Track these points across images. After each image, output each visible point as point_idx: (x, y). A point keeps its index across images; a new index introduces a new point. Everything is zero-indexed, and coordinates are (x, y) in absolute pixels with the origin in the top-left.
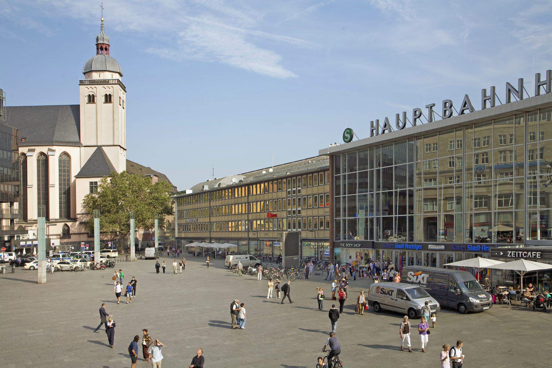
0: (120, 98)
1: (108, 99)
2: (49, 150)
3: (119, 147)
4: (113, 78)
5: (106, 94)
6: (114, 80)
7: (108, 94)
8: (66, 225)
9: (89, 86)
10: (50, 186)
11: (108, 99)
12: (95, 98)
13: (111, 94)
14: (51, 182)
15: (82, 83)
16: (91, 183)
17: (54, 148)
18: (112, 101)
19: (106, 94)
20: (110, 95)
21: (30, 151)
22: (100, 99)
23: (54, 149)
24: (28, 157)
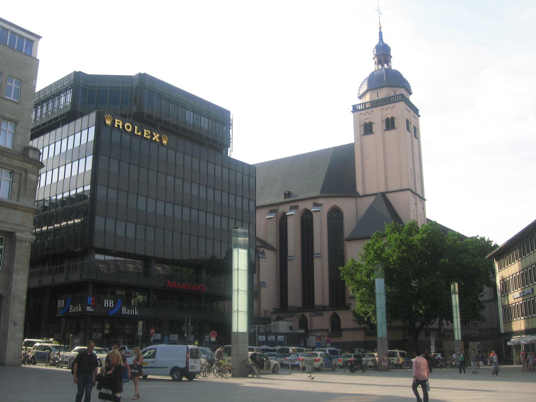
0: (408, 122)
1: (390, 124)
2: (315, 205)
3: (409, 192)
4: (396, 94)
5: (387, 118)
6: (397, 96)
8: (336, 314)
9: (364, 112)
10: (314, 256)
12: (373, 125)
13: (394, 117)
14: (316, 250)
17: (320, 201)
18: (396, 126)
19: (387, 118)
21: (292, 208)
22: (378, 127)
24: (288, 217)
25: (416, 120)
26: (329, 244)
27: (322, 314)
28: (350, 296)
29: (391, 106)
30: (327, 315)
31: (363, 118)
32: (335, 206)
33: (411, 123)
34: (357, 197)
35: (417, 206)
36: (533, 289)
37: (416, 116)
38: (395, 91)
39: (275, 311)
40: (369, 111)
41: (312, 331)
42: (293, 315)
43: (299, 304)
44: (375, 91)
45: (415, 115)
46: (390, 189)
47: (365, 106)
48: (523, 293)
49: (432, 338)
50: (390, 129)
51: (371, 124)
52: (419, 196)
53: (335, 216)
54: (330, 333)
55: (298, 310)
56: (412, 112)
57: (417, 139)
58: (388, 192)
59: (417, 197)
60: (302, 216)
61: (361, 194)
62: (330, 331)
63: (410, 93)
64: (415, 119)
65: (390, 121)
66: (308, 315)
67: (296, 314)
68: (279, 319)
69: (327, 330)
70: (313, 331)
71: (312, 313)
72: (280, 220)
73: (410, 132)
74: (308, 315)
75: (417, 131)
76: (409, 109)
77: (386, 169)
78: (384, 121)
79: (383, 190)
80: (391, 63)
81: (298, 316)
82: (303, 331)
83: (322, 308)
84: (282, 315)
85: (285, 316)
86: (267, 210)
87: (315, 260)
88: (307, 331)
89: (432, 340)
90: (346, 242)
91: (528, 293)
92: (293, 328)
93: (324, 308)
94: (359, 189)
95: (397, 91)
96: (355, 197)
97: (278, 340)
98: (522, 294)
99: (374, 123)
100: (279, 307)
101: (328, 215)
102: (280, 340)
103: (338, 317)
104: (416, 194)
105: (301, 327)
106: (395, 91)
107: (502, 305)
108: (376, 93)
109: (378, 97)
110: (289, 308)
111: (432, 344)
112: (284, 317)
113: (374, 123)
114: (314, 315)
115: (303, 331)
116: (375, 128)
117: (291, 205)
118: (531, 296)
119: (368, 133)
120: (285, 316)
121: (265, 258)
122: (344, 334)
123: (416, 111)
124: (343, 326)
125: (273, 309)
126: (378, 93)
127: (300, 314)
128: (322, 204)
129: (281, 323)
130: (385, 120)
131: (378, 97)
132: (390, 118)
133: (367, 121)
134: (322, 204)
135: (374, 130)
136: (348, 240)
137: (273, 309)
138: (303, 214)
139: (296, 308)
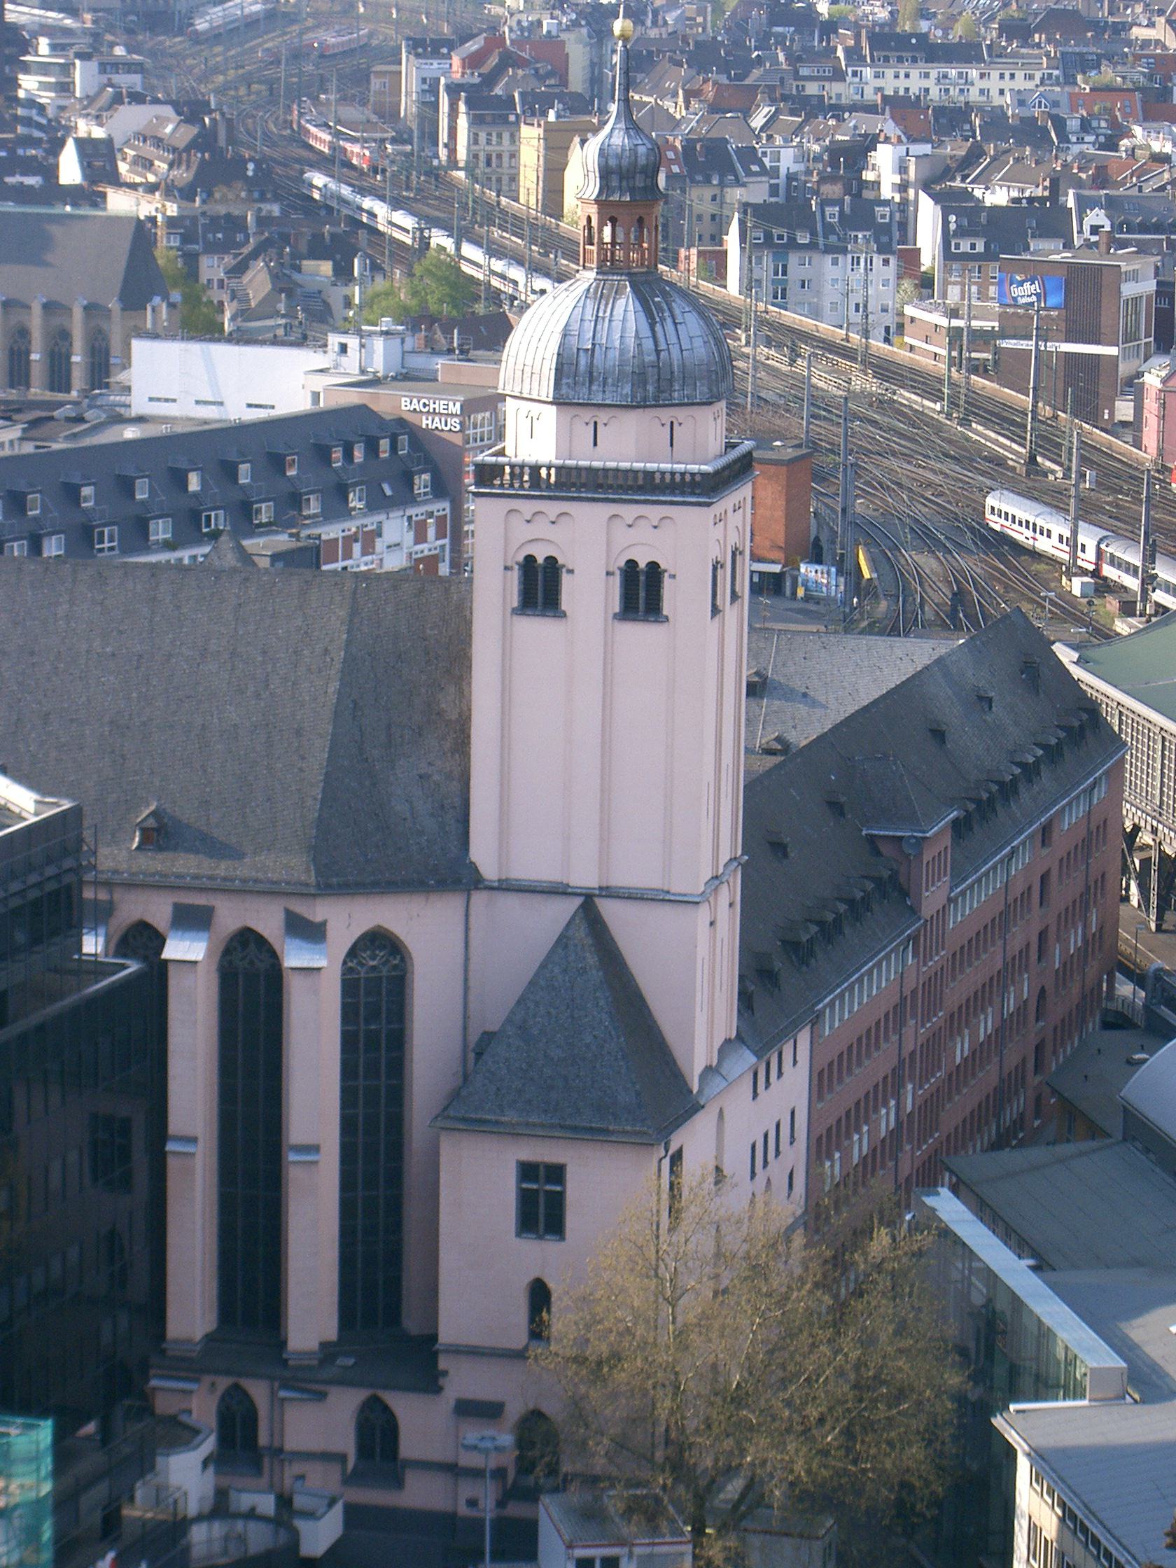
7: (642, 565)
10: (292, 1157)
11: (642, 594)
12: (565, 579)
13: (663, 566)
16: (527, 1171)
17: (319, 911)
20: (653, 566)
23: (318, 918)
31: (522, 532)
44: (587, 415)
46: (620, 879)
58: (609, 892)
60: (227, 951)
62: (351, 1462)
65: (642, 578)
67: (207, 1379)
69: (343, 1458)
74: (258, 1391)
77: (605, 790)
78: (618, 572)
79: (585, 877)
101: (345, 963)
103: (386, 1409)
109: (595, 444)
113: (571, 571)
116: (569, 588)
117: (176, 900)
124: (409, 1447)
126: (596, 423)
127: (224, 1383)
128: (324, 924)
130: (619, 568)
131: (595, 444)
132: (642, 565)
134: (324, 924)
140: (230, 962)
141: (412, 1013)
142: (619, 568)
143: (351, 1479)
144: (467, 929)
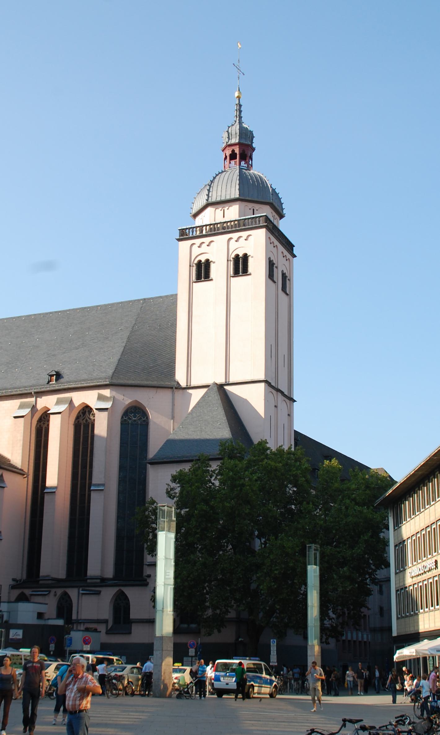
7: (241, 255)
12: (212, 265)
13: (248, 254)
14: (97, 477)
15: (184, 235)
19: (237, 256)
25: (287, 263)
26: (122, 468)
27: (98, 593)
28: (148, 562)
29: (244, 234)
30: (108, 594)
32: (136, 401)
33: (276, 267)
34: (176, 388)
35: (277, 410)
36: (436, 562)
37: (289, 256)
38: (253, 210)
39: (17, 585)
40: (207, 240)
41: (78, 622)
42: (47, 593)
43: (61, 574)
45: (286, 253)
47: (201, 231)
48: (423, 569)
49: (272, 640)
50: (241, 274)
51: (208, 263)
52: (282, 393)
53: (135, 420)
54: (109, 627)
55: (57, 583)
56: (281, 248)
57: (287, 294)
59: (280, 394)
61: (183, 384)
62: (110, 624)
63: (281, 216)
64: (287, 260)
66: (73, 593)
67: (53, 591)
68: (22, 598)
69: (106, 622)
70: (81, 623)
71: (81, 589)
72: (38, 421)
73: (275, 282)
74: (73, 593)
75: (288, 281)
76: (276, 243)
79: (221, 380)
80: (252, 160)
81: (55, 595)
82: (60, 622)
83: (99, 581)
84: (28, 592)
85: (34, 593)
86: (16, 402)
87: (93, 495)
88: (69, 620)
89: (272, 644)
90: (149, 466)
91: (429, 568)
92: (46, 616)
93: (103, 582)
94: (180, 377)
95: (257, 210)
96: (172, 388)
97: (11, 637)
98: (422, 570)
99: (214, 263)
100: (25, 577)
101: (122, 417)
102: (14, 637)
103: (126, 598)
104: (278, 390)
105: (59, 615)
106: (253, 210)
107: (396, 588)
108: (221, 210)
109: (224, 217)
110: (41, 580)
111: (272, 652)
112: (32, 595)
113: (214, 263)
114: (83, 594)
115: (60, 622)
118: (434, 572)
119: (203, 279)
120: (34, 593)
121: (4, 487)
122: (135, 629)
123: (289, 246)
124: (133, 615)
125: (14, 580)
127: (60, 591)
129: (22, 606)
130: (233, 258)
131: (224, 217)
132: (241, 255)
133: (203, 259)
135: (213, 274)
136: (152, 463)
137: (14, 580)
138: (79, 412)
139: (53, 579)
140: (78, 422)
141: (149, 435)
142: (233, 258)
143: (109, 632)
144: (173, 405)
